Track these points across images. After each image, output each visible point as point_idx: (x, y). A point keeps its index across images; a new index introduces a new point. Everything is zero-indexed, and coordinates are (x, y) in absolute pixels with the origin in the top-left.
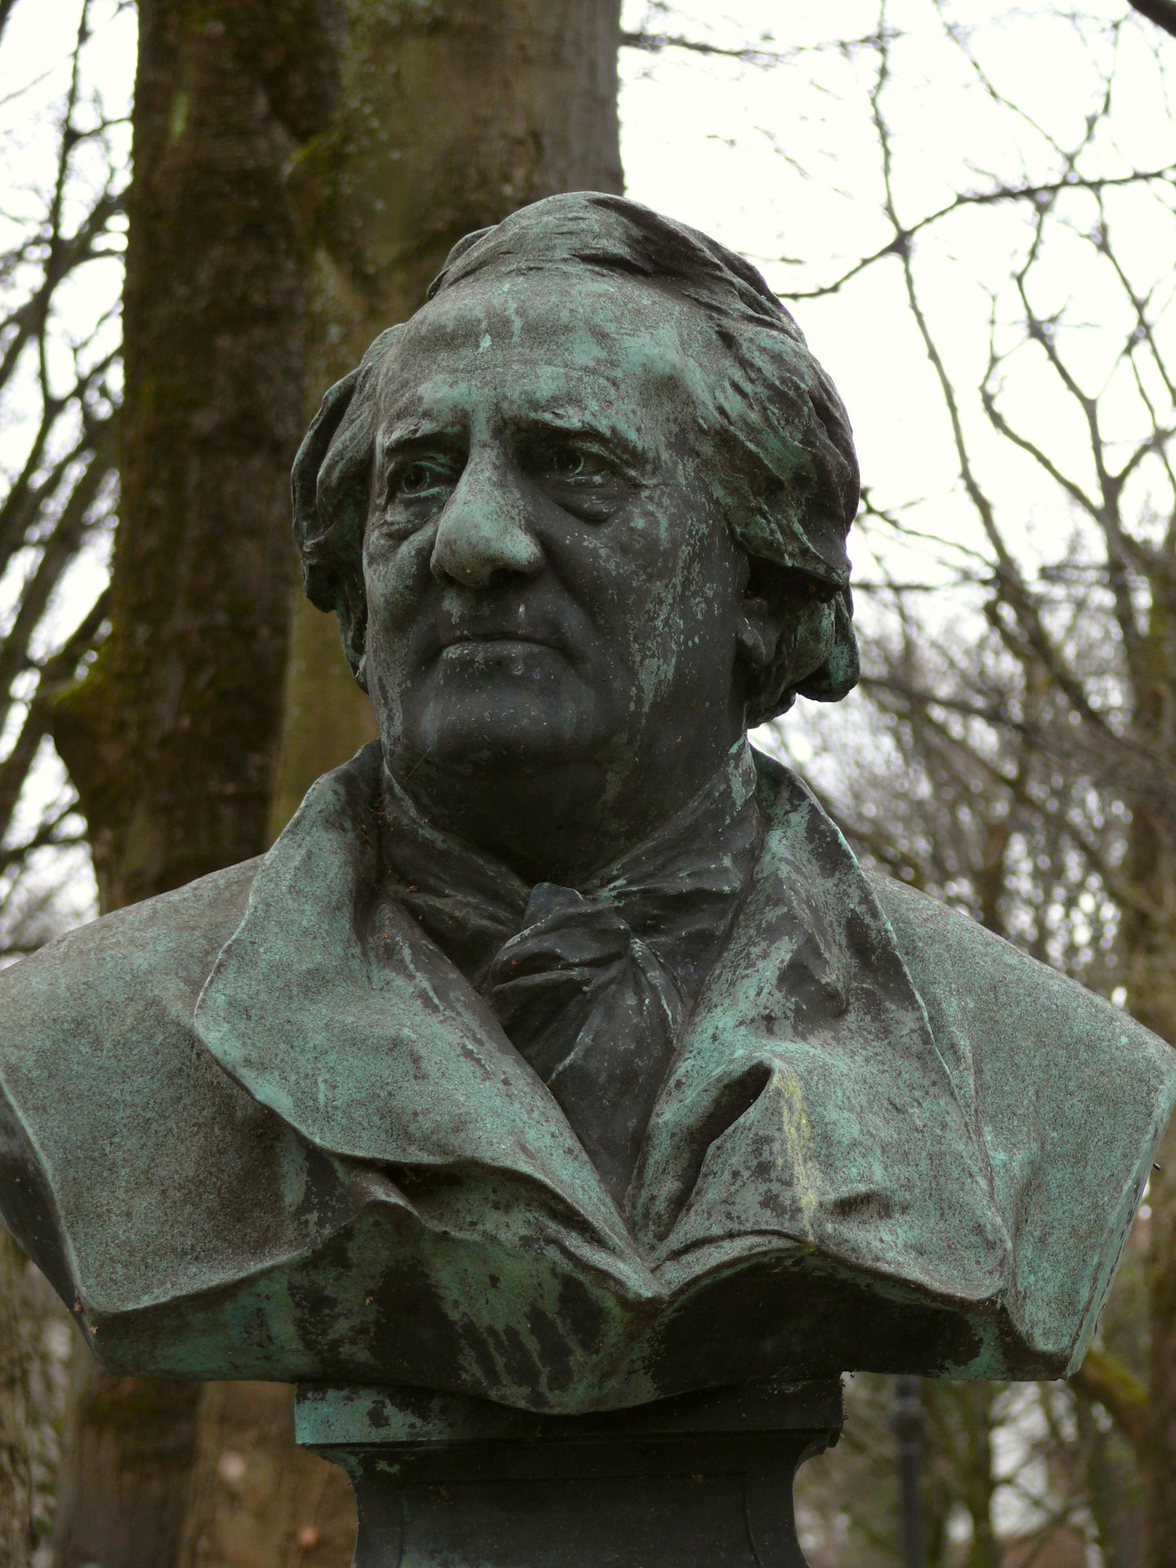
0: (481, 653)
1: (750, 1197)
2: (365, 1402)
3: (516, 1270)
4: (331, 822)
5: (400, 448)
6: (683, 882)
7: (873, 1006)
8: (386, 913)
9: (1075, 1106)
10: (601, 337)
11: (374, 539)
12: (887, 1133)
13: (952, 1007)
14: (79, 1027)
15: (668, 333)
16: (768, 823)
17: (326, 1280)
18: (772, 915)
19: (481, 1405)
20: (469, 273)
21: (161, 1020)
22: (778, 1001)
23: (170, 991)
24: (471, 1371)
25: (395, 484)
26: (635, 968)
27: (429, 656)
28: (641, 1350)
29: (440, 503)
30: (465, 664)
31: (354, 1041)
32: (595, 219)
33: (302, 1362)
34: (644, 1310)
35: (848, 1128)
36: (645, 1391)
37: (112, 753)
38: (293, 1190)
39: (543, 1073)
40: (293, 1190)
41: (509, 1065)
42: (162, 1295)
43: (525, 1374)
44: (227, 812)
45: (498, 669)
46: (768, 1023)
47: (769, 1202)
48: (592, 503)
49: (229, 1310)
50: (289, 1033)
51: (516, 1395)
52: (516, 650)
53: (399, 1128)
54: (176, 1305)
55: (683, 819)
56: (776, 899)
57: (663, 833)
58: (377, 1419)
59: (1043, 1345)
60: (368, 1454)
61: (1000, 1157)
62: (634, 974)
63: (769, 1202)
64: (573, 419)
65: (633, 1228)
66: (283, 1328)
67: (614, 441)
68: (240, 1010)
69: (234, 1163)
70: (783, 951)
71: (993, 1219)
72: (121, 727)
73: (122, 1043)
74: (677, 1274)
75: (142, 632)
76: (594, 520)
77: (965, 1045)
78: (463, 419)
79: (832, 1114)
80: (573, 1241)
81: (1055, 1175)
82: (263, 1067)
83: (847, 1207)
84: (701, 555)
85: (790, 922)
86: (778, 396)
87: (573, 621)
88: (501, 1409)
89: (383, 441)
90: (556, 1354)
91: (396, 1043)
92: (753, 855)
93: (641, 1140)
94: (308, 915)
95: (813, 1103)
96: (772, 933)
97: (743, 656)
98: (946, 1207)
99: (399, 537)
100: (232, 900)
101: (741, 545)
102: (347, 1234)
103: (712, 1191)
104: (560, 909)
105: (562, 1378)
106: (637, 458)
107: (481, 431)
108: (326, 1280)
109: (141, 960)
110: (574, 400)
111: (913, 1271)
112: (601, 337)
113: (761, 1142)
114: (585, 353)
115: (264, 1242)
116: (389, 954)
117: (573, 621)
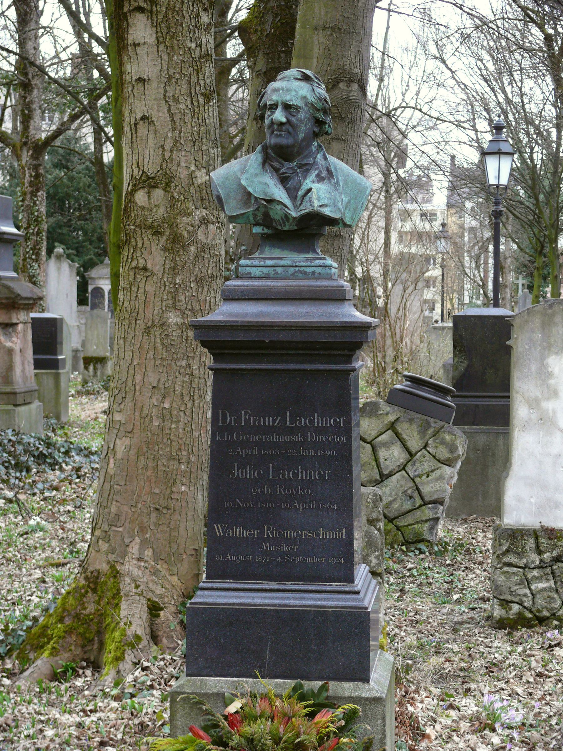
0: (278, 133)
1: (309, 204)
2: (262, 227)
3: (279, 212)
4: (260, 153)
5: (270, 105)
6: (305, 162)
7: (329, 179)
8: (267, 165)
9: (356, 192)
10: (296, 91)
11: (266, 116)
12: (328, 196)
13: (340, 179)
14: (227, 178)
15: (305, 90)
16: (318, 153)
17: (257, 213)
18: (316, 167)
20: (280, 79)
21: (237, 178)
22: (315, 179)
23: (239, 174)
24: (274, 224)
25: (269, 109)
26: (298, 174)
27: (272, 132)
28: (295, 223)
29: (274, 112)
30: (277, 134)
31: (261, 183)
32: (297, 73)
33: (254, 222)
34: (295, 218)
35: (322, 195)
36: (295, 228)
37: (254, 38)
39: (284, 187)
41: (280, 187)
42: (236, 214)
43: (281, 225)
44: (282, 55)
45: (281, 135)
46: (314, 182)
47: (311, 205)
48: (294, 114)
49: (245, 216)
50: (252, 182)
51: (279, 228)
52: (283, 133)
53: (266, 194)
54: (238, 215)
55: (305, 154)
56: (317, 165)
57: (302, 156)
58: (263, 230)
59: (348, 223)
60: (262, 234)
61: (344, 199)
63: (311, 205)
64: (291, 103)
65: (295, 208)
66: (251, 218)
67: (297, 106)
68: (247, 179)
69: (246, 197)
70: (317, 172)
71: (341, 207)
72: (256, 31)
73: (232, 180)
74: (299, 214)
75: (262, 5)
76: (294, 116)
77: (341, 184)
78: (278, 102)
79: (320, 194)
80: (286, 209)
81: (352, 201)
82: (249, 186)
83: (321, 206)
84: (308, 119)
85: (318, 168)
86: (319, 99)
87: (291, 129)
88: (278, 229)
89: (268, 103)
90: (284, 223)
91: (266, 183)
92: (315, 158)
93: (296, 196)
95: (317, 193)
96: (315, 170)
97: (314, 132)
98: (335, 206)
99: (269, 116)
100: (247, 161)
101: (315, 117)
102: (259, 207)
103: (304, 203)
104: (288, 166)
105: (285, 226)
106: (300, 108)
107: (280, 104)
108: (257, 213)
109: (235, 169)
110: (292, 100)
112: (296, 91)
113: (310, 198)
114: (293, 93)
115: (249, 207)
116: (266, 171)
117: (291, 129)
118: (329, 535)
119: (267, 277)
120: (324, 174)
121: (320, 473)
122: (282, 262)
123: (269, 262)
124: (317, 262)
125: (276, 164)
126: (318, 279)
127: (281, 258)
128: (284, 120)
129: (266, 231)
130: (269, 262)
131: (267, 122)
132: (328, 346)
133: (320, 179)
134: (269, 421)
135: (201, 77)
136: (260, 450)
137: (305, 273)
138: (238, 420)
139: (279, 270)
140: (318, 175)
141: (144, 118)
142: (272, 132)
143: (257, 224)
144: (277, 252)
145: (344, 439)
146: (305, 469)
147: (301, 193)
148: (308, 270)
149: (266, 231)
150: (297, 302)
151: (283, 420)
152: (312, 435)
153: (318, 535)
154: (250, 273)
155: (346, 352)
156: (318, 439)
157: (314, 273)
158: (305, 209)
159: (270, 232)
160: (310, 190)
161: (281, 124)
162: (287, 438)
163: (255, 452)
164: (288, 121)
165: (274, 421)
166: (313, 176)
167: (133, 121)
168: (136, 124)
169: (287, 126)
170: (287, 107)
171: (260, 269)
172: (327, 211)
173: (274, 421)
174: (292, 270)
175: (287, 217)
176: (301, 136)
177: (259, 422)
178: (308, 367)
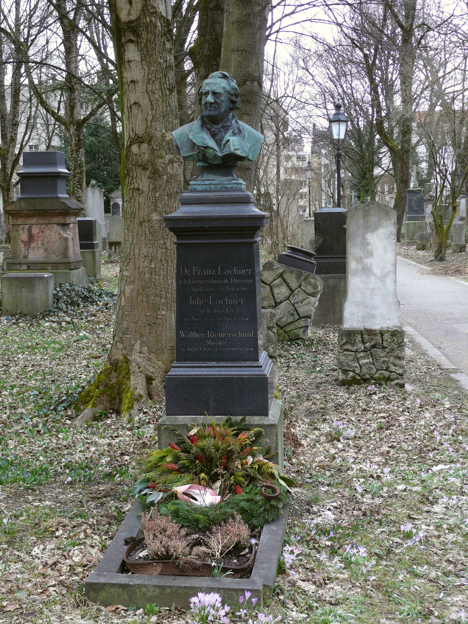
3: (212, 154)
6: (225, 125)
13: (246, 134)
14: (181, 135)
19: (210, 163)
23: (188, 132)
27: (206, 108)
31: (200, 137)
34: (220, 157)
35: (235, 143)
36: (221, 162)
37: (198, 57)
38: (196, 148)
39: (214, 139)
40: (196, 148)
41: (212, 139)
44: (214, 67)
46: (230, 136)
51: (212, 162)
53: (203, 143)
60: (202, 166)
62: (221, 132)
64: (217, 91)
66: (196, 157)
68: (193, 135)
70: (232, 130)
72: (199, 53)
75: (202, 39)
81: (253, 147)
87: (217, 106)
93: (221, 144)
94: (198, 127)
97: (230, 108)
100: (193, 125)
111: (240, 154)
114: (218, 86)
117: (217, 106)
118: (244, 335)
119: (206, 191)
120: (236, 131)
121: (238, 301)
122: (214, 182)
123: (206, 182)
124: (234, 182)
125: (209, 126)
126: (234, 191)
127: (213, 180)
128: (213, 101)
129: (204, 164)
130: (206, 182)
131: (203, 102)
132: (241, 229)
133: (234, 134)
134: (209, 272)
135: (167, 79)
136: (204, 289)
137: (227, 188)
138: (191, 272)
139: (212, 187)
140: (233, 132)
141: (135, 103)
142: (206, 108)
143: (199, 161)
144: (211, 177)
145: (251, 281)
146: (230, 298)
147: (223, 143)
148: (229, 186)
149: (204, 164)
150: (223, 205)
151: (217, 272)
152: (233, 279)
153: (238, 335)
154: (196, 189)
155: (251, 232)
156: (237, 281)
157: (232, 188)
158: (226, 152)
159: (207, 165)
160: (228, 141)
161: (211, 103)
162: (219, 282)
163: (202, 290)
164: (215, 102)
165: (212, 272)
166: (230, 132)
167: (129, 105)
168: (131, 107)
169: (215, 105)
170: (214, 93)
171: (201, 186)
172: (239, 153)
173: (212, 272)
174: (219, 186)
175: (216, 156)
176: (223, 110)
177: (203, 273)
178: (230, 241)
